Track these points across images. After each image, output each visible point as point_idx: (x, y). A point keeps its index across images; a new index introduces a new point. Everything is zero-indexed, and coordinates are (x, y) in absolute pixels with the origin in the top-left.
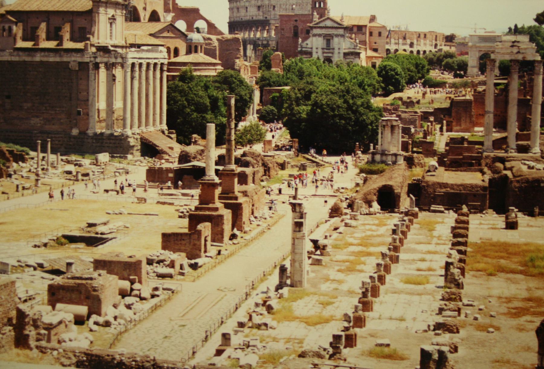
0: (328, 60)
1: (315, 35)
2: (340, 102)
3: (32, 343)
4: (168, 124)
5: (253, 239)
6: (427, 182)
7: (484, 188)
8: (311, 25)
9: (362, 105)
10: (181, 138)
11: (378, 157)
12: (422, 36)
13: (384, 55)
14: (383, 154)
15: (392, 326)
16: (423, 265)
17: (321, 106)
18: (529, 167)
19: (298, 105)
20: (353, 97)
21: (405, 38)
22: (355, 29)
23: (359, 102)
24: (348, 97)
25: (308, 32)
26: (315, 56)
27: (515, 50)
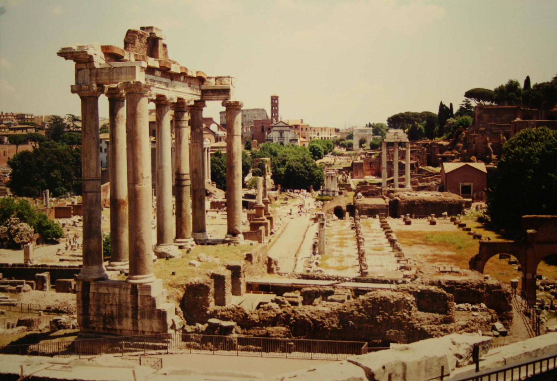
0: (282, 144)
1: (274, 131)
2: (302, 165)
3: (275, 271)
4: (212, 179)
5: (280, 235)
6: (358, 204)
7: (387, 206)
8: (272, 125)
9: (313, 166)
10: (219, 186)
11: (325, 193)
12: (323, 129)
13: (309, 140)
14: (328, 191)
15: (379, 269)
16: (377, 242)
17: (292, 168)
18: (408, 195)
19: (279, 167)
20: (308, 163)
21: (314, 131)
22: (294, 127)
23: (311, 165)
24: (305, 163)
25: (269, 130)
26: (275, 142)
27: (396, 137)
